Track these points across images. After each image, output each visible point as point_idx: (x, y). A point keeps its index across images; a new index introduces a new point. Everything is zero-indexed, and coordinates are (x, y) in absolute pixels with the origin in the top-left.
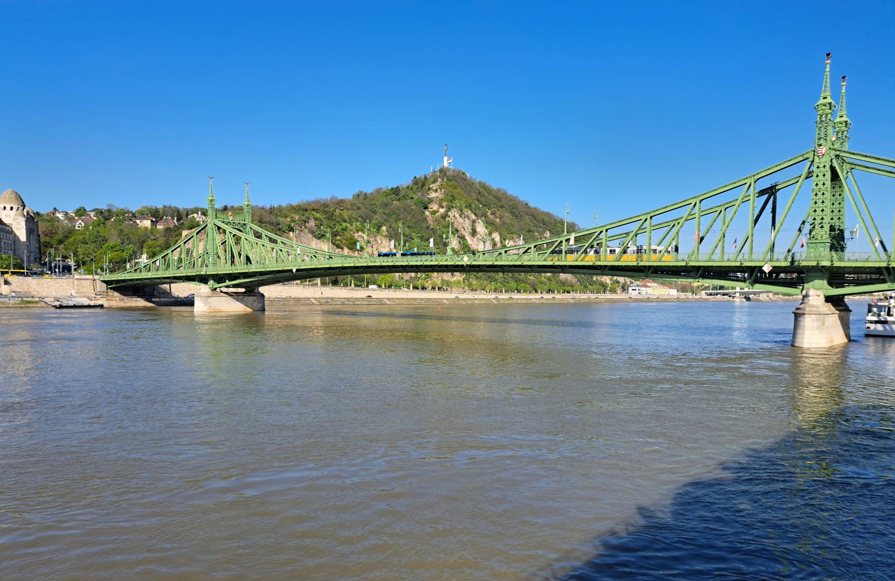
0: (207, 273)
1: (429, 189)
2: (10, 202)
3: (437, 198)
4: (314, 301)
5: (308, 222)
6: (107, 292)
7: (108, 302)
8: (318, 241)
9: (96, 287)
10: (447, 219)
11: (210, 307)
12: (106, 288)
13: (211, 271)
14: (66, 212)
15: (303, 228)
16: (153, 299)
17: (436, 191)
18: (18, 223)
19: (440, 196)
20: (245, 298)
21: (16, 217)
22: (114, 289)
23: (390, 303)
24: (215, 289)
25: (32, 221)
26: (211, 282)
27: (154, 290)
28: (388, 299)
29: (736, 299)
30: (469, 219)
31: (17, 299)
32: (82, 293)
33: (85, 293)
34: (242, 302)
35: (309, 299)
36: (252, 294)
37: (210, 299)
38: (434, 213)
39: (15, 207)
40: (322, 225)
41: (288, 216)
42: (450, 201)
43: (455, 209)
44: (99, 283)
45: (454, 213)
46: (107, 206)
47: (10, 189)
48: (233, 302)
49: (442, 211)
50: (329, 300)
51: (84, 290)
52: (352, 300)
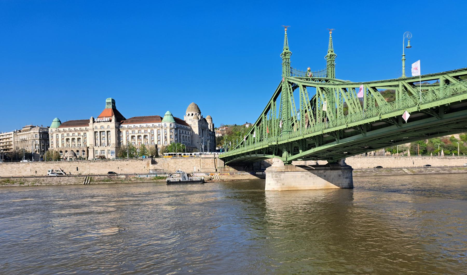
0: (279, 143)
2: (191, 110)
4: (406, 171)
6: (225, 168)
7: (220, 176)
9: (217, 164)
12: (224, 164)
13: (285, 139)
14: (250, 124)
16: (257, 173)
18: (195, 124)
20: (328, 172)
24: (290, 162)
25: (202, 122)
31: (153, 176)
32: (206, 169)
33: (208, 169)
35: (401, 169)
36: (335, 167)
37: (283, 175)
39: (194, 113)
44: (218, 160)
48: (312, 178)
51: (208, 167)
52: (447, 168)
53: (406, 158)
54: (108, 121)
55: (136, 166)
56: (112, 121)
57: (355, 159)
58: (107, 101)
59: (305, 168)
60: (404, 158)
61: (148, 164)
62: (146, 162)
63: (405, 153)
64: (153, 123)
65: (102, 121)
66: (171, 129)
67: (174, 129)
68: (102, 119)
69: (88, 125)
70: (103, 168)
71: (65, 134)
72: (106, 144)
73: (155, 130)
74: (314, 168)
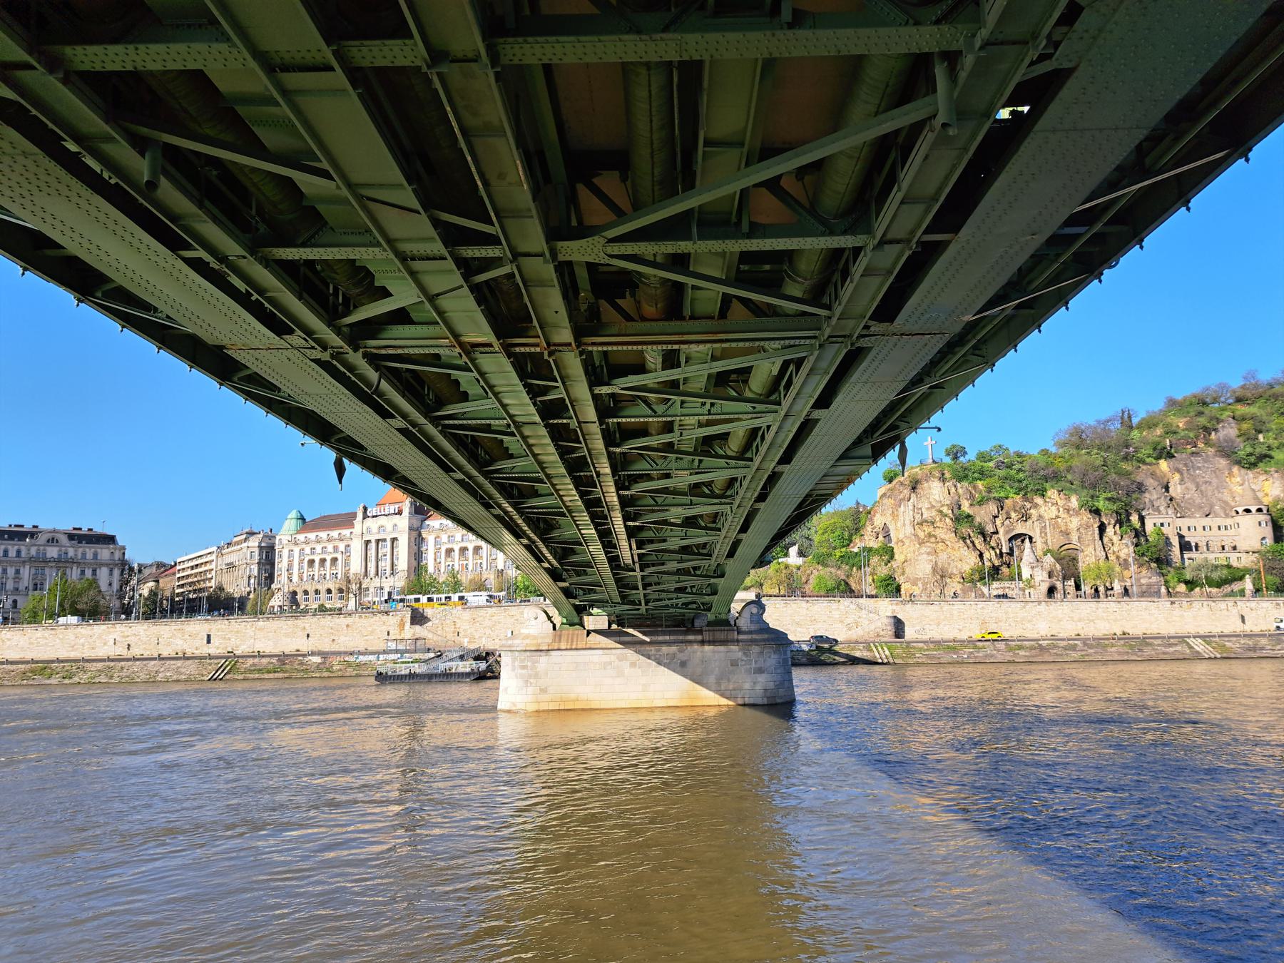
4: (1199, 646)
5: (1216, 430)
8: (1250, 474)
15: (1201, 445)
35: (1182, 639)
36: (721, 636)
40: (1260, 432)
41: (1156, 425)
50: (1263, 641)
53: (1213, 604)
57: (1027, 607)
59: (618, 639)
60: (1205, 603)
62: (398, 618)
63: (1236, 587)
69: (352, 526)
70: (287, 635)
71: (308, 550)
72: (388, 571)
74: (647, 639)
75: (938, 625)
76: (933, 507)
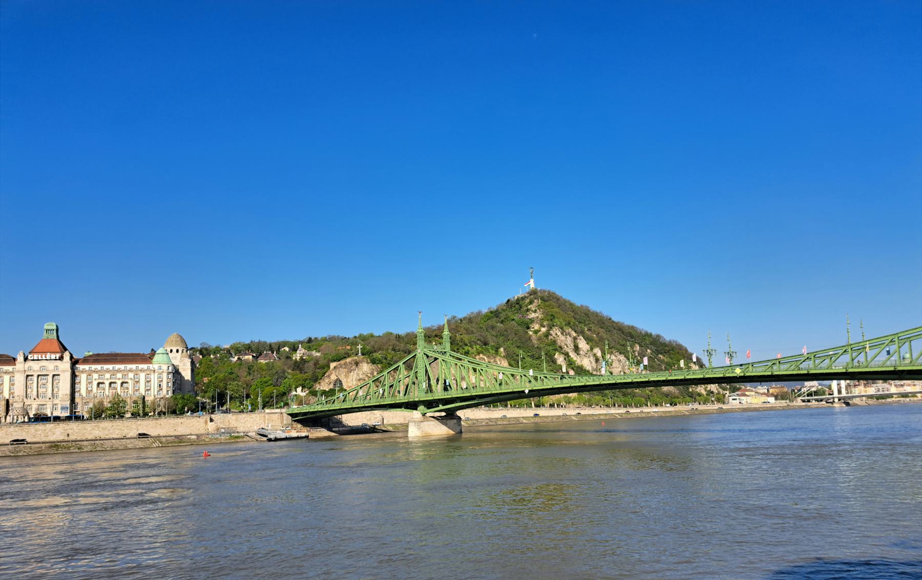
1: (528, 310)
2: (176, 345)
3: (537, 318)
6: (292, 424)
10: (550, 337)
11: (422, 431)
16: (333, 429)
17: (535, 312)
19: (540, 317)
21: (182, 359)
22: (298, 421)
23: (527, 422)
26: (421, 408)
27: (329, 420)
28: (523, 418)
29: (835, 405)
30: (570, 336)
34: (446, 425)
38: (536, 332)
42: (551, 320)
43: (556, 328)
44: (285, 415)
45: (556, 332)
46: (201, 344)
47: (175, 334)
49: (544, 330)
50: (475, 421)
54: (56, 360)
55: (192, 424)
56: (64, 360)
58: (46, 327)
61: (206, 422)
62: (204, 419)
64: (148, 364)
65: (44, 358)
66: (169, 373)
67: (172, 374)
68: (44, 356)
70: (152, 428)
73: (142, 376)
75: (393, 418)
76: (364, 374)
